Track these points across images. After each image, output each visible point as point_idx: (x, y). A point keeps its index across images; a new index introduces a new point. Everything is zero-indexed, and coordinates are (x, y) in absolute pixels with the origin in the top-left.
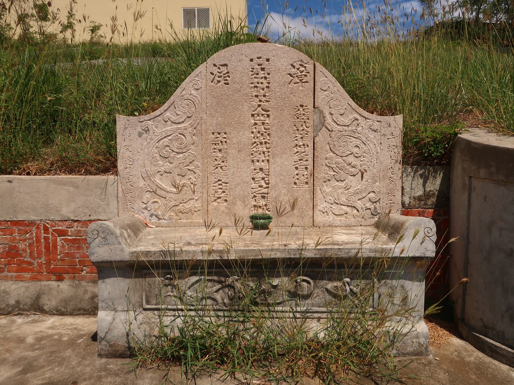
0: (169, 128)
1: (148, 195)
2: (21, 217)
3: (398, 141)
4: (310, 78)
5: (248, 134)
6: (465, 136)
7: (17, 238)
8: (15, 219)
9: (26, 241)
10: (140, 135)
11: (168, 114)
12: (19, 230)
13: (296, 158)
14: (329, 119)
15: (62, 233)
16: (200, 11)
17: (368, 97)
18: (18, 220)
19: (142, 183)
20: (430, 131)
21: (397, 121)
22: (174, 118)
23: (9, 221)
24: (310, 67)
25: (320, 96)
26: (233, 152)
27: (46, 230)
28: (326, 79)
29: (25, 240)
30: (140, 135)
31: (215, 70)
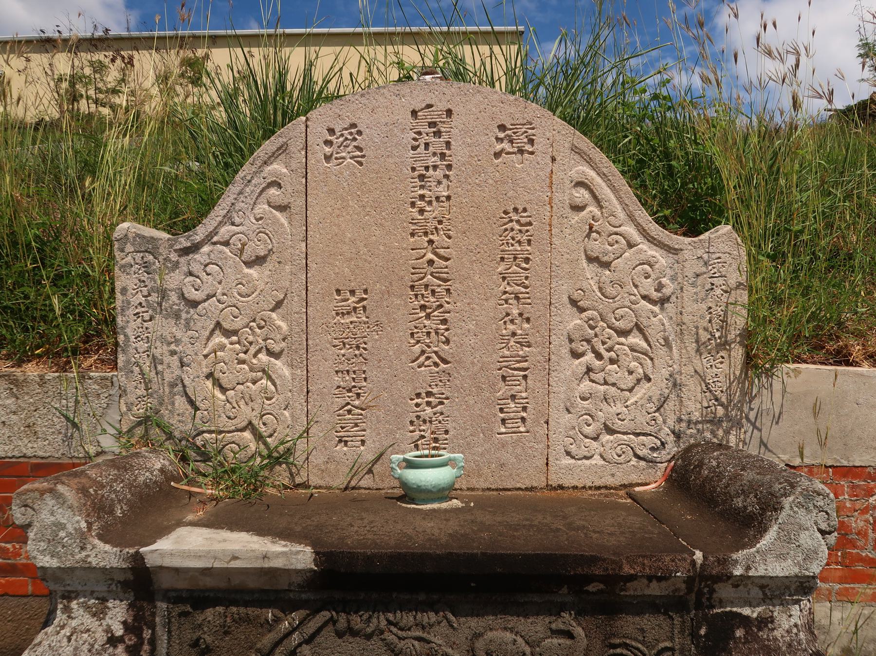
2: (858, 460)
7: (848, 505)
8: (845, 463)
9: (867, 513)
12: (853, 487)
18: (851, 464)
23: (830, 467)
29: (865, 511)
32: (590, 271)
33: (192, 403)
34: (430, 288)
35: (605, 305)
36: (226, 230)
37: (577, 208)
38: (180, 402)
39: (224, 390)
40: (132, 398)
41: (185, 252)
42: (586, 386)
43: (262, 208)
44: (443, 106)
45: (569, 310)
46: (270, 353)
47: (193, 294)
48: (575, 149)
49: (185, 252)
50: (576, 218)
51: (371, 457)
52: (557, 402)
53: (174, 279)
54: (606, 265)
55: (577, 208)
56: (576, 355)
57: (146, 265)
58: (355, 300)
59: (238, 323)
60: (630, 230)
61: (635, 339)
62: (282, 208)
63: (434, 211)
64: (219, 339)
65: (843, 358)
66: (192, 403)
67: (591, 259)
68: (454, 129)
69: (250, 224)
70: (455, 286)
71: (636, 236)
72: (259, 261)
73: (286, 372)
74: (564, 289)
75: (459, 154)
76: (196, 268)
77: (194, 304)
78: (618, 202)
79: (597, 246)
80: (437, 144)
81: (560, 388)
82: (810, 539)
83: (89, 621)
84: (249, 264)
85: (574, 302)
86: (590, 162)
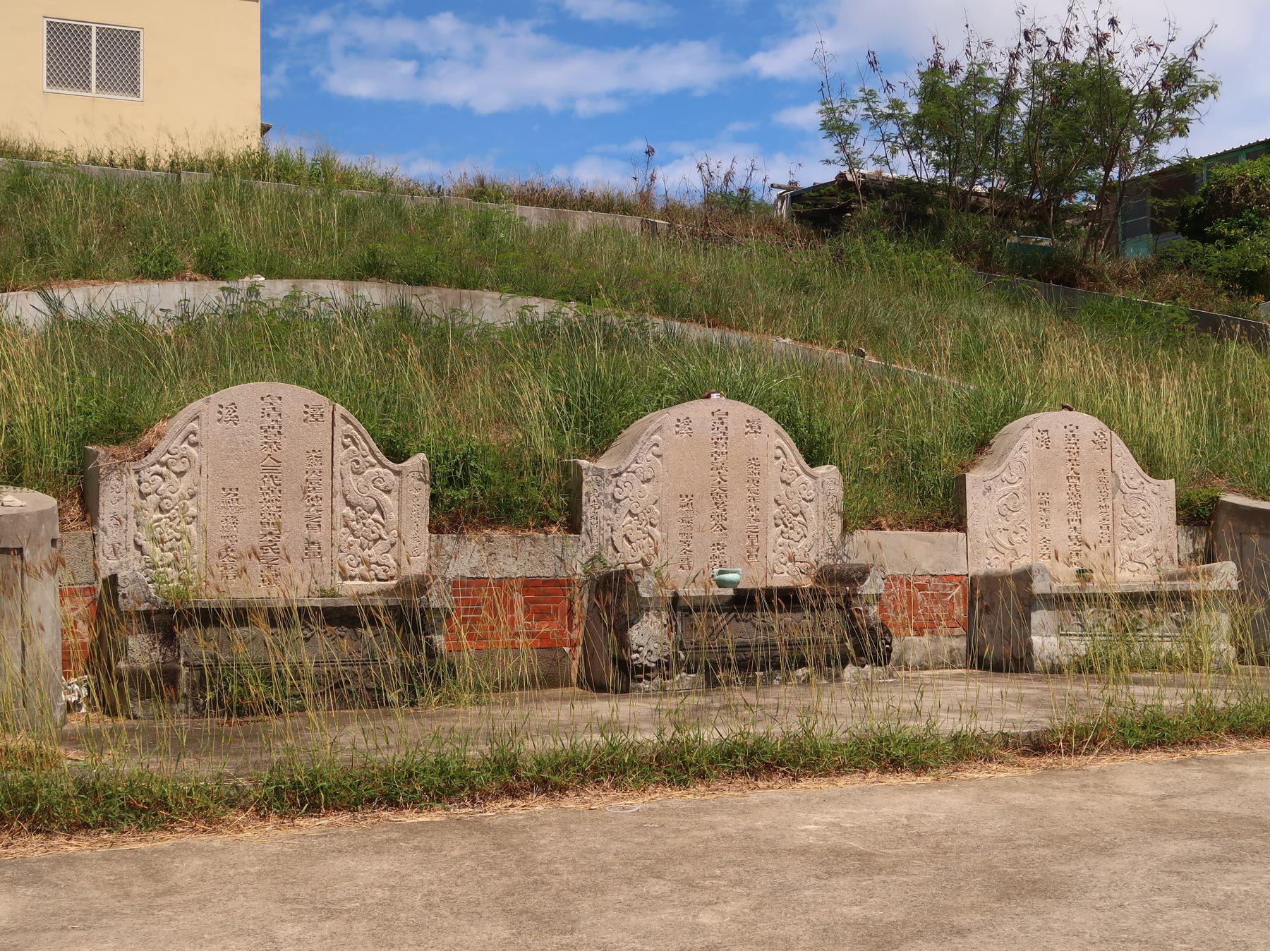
0: (1007, 487)
1: (990, 551)
3: (1173, 503)
4: (1107, 445)
5: (1064, 494)
6: (1223, 498)
10: (984, 494)
11: (1004, 475)
13: (1101, 518)
14: (1123, 484)
15: (921, 588)
16: (106, 34)
17: (1153, 465)
19: (986, 540)
20: (1199, 494)
21: (1170, 484)
22: (1009, 479)
24: (1108, 435)
25: (1116, 460)
26: (1054, 511)
27: (908, 584)
28: (1120, 447)
30: (984, 494)
31: (1039, 435)
32: (783, 486)
33: (616, 549)
34: (719, 496)
35: (788, 503)
36: (634, 466)
37: (777, 458)
38: (610, 548)
39: (630, 542)
40: (588, 547)
41: (615, 476)
42: (781, 540)
43: (650, 456)
44: (724, 411)
45: (774, 505)
46: (651, 524)
47: (618, 496)
48: (777, 432)
49: (615, 476)
50: (777, 463)
51: (693, 574)
52: (770, 547)
53: (610, 489)
54: (789, 484)
55: (777, 458)
56: (777, 525)
57: (598, 482)
58: (688, 501)
59: (639, 510)
60: (797, 468)
61: (800, 518)
62: (658, 456)
63: (721, 459)
64: (629, 518)
65: (878, 527)
66: (616, 549)
67: (783, 482)
68: (729, 421)
69: (644, 464)
70: (728, 493)
71: (800, 472)
72: (648, 481)
73: (658, 534)
74: (772, 496)
75: (730, 433)
76: (620, 484)
77: (618, 501)
78: (795, 458)
79: (785, 476)
80: (722, 428)
81: (771, 541)
82: (879, 581)
83: (655, 619)
84: (643, 482)
85: (776, 501)
86: (782, 437)
